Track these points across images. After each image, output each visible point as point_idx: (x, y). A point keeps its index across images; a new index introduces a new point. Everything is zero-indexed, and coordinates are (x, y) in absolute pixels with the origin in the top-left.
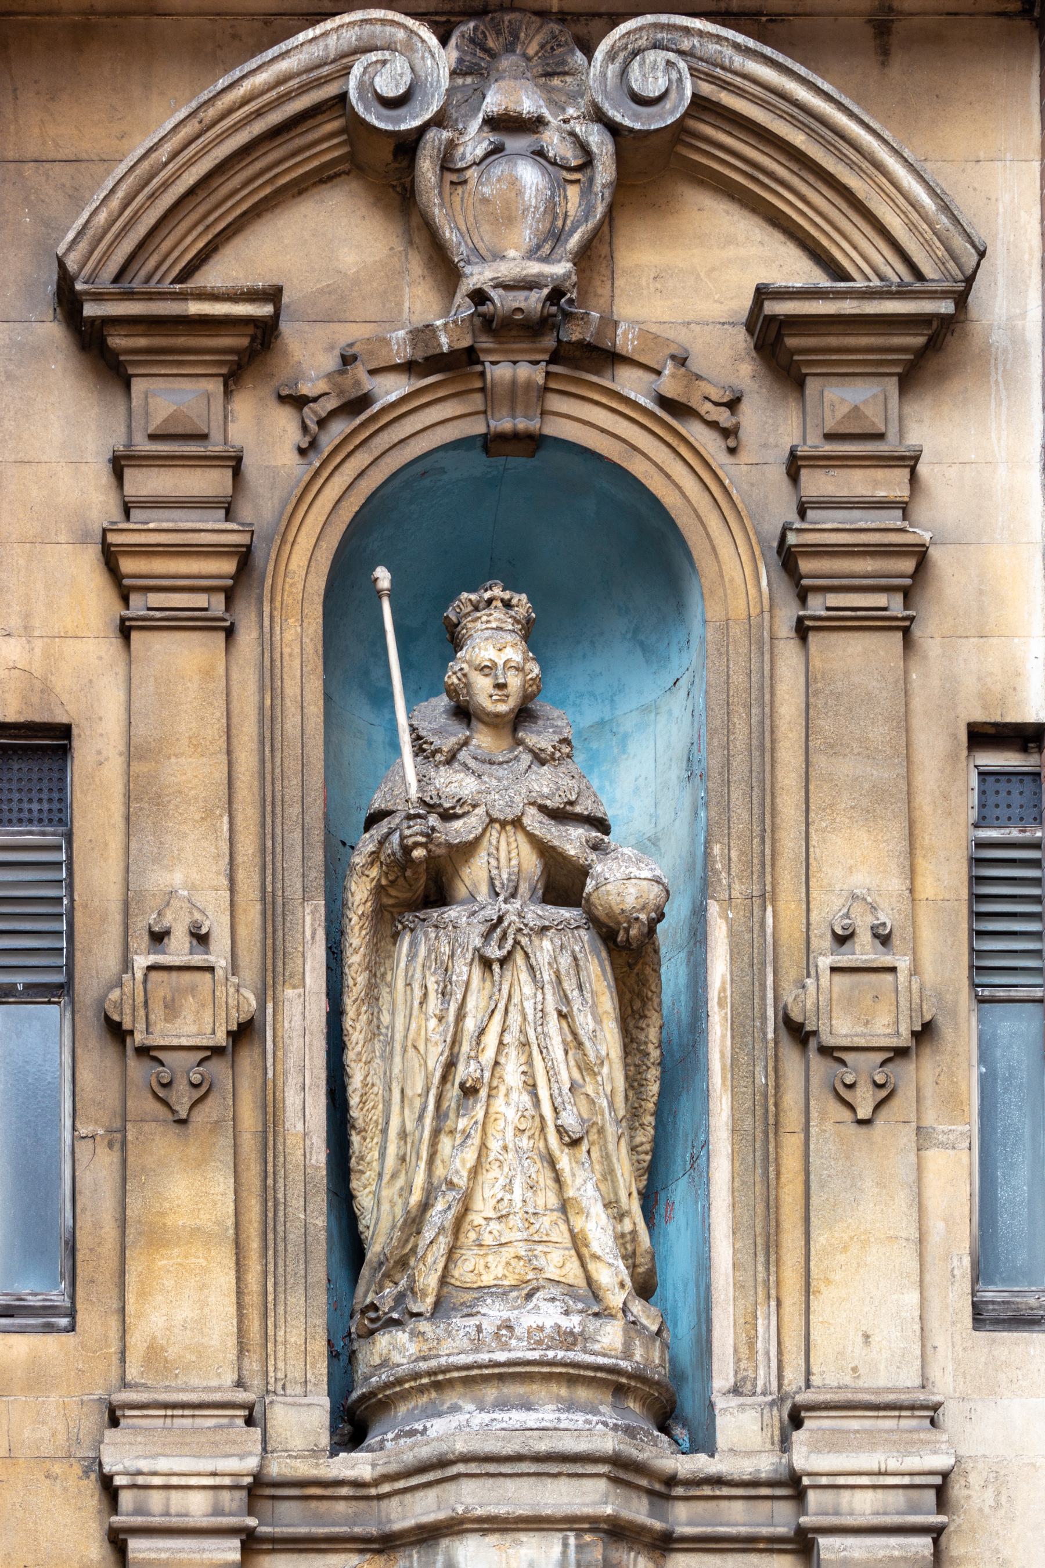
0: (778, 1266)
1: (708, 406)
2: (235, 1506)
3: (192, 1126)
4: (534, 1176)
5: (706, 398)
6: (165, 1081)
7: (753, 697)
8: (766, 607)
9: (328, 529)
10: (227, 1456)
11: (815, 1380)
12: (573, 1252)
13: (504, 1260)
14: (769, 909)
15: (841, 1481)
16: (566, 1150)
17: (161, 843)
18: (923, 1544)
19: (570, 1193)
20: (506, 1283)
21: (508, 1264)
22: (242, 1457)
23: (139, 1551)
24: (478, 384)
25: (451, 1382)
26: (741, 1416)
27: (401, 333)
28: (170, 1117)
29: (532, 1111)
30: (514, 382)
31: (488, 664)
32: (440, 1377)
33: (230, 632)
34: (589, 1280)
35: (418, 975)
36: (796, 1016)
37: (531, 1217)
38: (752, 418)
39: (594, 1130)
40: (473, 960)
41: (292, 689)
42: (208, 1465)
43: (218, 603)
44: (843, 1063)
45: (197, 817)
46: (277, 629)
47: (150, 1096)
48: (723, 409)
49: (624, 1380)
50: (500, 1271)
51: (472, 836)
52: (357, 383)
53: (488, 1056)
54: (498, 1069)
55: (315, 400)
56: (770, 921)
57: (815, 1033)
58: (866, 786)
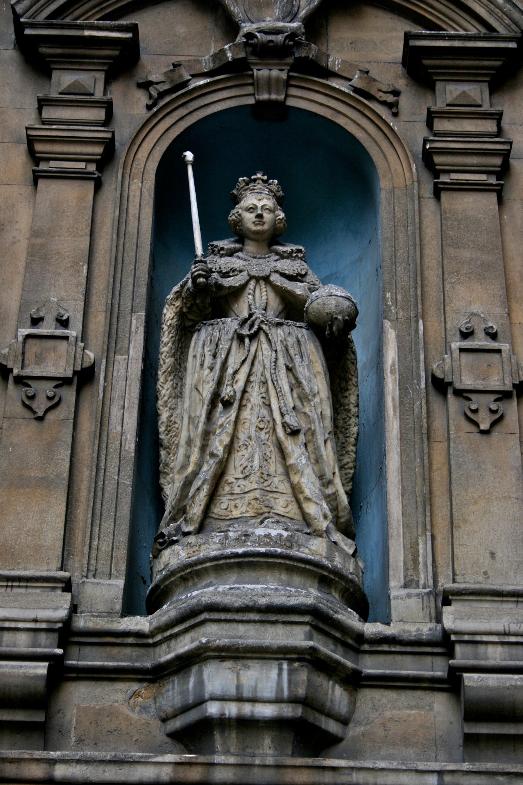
1: (381, 94)
2: (48, 642)
3: (46, 422)
4: (268, 453)
5: (380, 90)
6: (30, 395)
7: (409, 222)
8: (415, 179)
9: (161, 142)
10: (44, 608)
11: (458, 578)
12: (293, 499)
13: (247, 502)
14: (421, 322)
15: (478, 638)
16: (289, 438)
17: (44, 277)
19: (291, 461)
20: (248, 515)
21: (249, 504)
22: (56, 609)
24: (250, 81)
25: (206, 569)
26: (408, 600)
27: (207, 57)
28: (32, 416)
29: (268, 418)
31: (251, 206)
32: (199, 567)
34: (305, 516)
35: (200, 350)
36: (439, 374)
37: (265, 476)
38: (405, 102)
39: (310, 433)
40: (233, 338)
41: (133, 211)
42: (31, 614)
43: (92, 168)
44: (469, 399)
45: (68, 265)
47: (19, 404)
48: (389, 95)
49: (326, 573)
50: (244, 509)
51: (237, 285)
52: (181, 76)
53: (240, 385)
54: (247, 395)
55: (157, 83)
56: (421, 327)
57: (451, 384)
58: (479, 263)
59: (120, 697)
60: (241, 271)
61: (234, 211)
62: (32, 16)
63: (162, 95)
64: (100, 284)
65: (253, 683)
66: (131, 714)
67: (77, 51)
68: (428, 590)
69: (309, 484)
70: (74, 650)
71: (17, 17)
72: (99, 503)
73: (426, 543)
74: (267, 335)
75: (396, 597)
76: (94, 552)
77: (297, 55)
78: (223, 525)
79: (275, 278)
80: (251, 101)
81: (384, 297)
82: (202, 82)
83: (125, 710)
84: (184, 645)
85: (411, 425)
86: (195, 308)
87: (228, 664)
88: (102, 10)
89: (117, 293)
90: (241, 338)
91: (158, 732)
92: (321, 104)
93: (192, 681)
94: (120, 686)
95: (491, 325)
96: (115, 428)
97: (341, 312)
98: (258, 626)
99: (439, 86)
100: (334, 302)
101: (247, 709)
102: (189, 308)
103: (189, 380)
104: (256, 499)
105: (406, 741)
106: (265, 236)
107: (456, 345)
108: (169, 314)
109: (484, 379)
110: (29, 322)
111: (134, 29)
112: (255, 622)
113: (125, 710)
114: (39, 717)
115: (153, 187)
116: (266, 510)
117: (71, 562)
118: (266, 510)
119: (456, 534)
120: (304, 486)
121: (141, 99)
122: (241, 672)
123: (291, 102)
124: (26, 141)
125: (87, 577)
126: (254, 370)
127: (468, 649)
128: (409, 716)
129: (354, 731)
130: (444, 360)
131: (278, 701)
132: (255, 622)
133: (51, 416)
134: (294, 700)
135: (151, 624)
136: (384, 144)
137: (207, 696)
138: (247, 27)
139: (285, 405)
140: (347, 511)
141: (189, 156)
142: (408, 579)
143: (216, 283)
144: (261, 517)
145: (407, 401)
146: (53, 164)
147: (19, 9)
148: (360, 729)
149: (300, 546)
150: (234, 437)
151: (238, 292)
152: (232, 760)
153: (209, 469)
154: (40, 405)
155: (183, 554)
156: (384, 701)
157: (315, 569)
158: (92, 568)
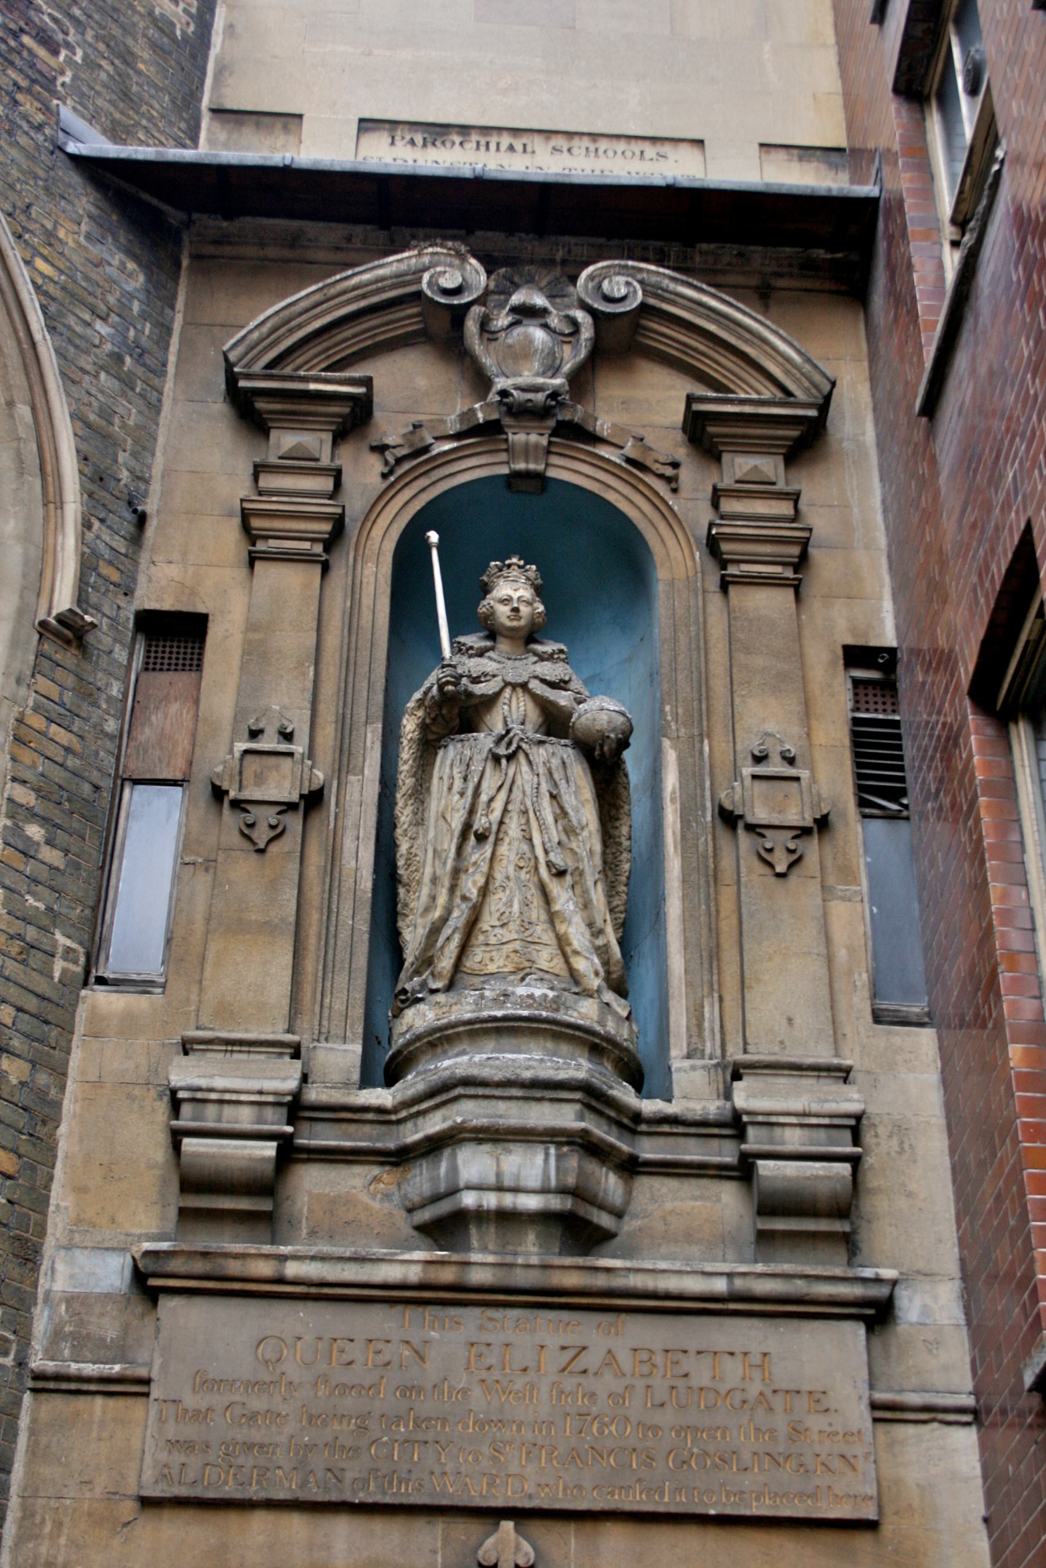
0: (719, 974)
1: (658, 466)
2: (276, 1117)
3: (268, 855)
5: (657, 461)
8: (699, 569)
9: (398, 518)
10: (271, 1078)
11: (750, 1048)
14: (706, 742)
15: (774, 1119)
16: (554, 879)
18: (844, 1169)
19: (556, 907)
20: (506, 970)
21: (508, 956)
23: (190, 1145)
24: (504, 446)
25: (458, 1034)
26: (692, 1073)
27: (453, 417)
28: (252, 848)
29: (529, 855)
30: (527, 443)
32: (450, 1032)
33: (326, 568)
34: (573, 973)
35: (447, 770)
36: (728, 805)
37: (526, 925)
38: (686, 475)
40: (486, 760)
41: (367, 601)
42: (256, 1085)
43: (318, 548)
44: (763, 836)
46: (359, 567)
47: (237, 833)
49: (597, 1041)
50: (501, 963)
52: (422, 439)
53: (496, 815)
54: (504, 827)
55: (394, 447)
56: (706, 749)
57: (741, 817)
59: (358, 1182)
60: (494, 676)
61: (485, 602)
62: (248, 365)
63: (399, 461)
64: (329, 689)
65: (515, 1170)
66: (371, 1202)
67: (299, 406)
68: (714, 1061)
69: (577, 934)
70: (305, 1126)
71: (229, 366)
72: (331, 952)
73: (712, 1005)
74: (527, 755)
75: (679, 1070)
76: (326, 1011)
77: (560, 418)
78: (476, 981)
79: (535, 685)
80: (505, 470)
81: (662, 711)
82: (447, 446)
83: (364, 1198)
84: (434, 1124)
85: (694, 864)
86: (440, 719)
87: (486, 1147)
88: (328, 357)
89: (349, 700)
90: (496, 759)
91: (404, 1225)
92: (587, 476)
93: (443, 1167)
94: (358, 1169)
95: (788, 747)
96: (348, 862)
97: (614, 730)
98: (521, 1103)
99: (726, 458)
100: (605, 718)
101: (509, 1200)
102: (434, 719)
103: (434, 806)
104: (516, 951)
105: (689, 1238)
106: (523, 633)
107: (748, 770)
108: (410, 726)
109: (780, 812)
110: (246, 735)
111: (368, 382)
112: (517, 1098)
113: (364, 1198)
114: (264, 1205)
115: (390, 572)
116: (527, 964)
117: (298, 1022)
118: (527, 964)
119: (747, 996)
120: (571, 937)
121: (375, 465)
122: (502, 1157)
123: (552, 473)
124: (239, 514)
125: (318, 1041)
126: (513, 796)
127: (763, 1131)
128: (693, 1208)
129: (629, 1225)
130: (733, 788)
131: (544, 1191)
132: (517, 1098)
133: (274, 848)
134: (563, 1191)
135: (394, 1097)
136: (662, 526)
137: (462, 1184)
138: (501, 383)
139: (550, 841)
140: (620, 965)
141: (433, 536)
142: (693, 1046)
143: (466, 690)
144: (523, 973)
145: (690, 836)
146: (272, 543)
147: (232, 357)
148: (637, 1223)
149: (567, 1008)
150: (489, 878)
151: (490, 701)
152: (490, 1259)
153: (459, 916)
154: (262, 835)
155: (431, 1015)
156: (664, 1190)
157: (586, 1036)
158: (324, 1030)
